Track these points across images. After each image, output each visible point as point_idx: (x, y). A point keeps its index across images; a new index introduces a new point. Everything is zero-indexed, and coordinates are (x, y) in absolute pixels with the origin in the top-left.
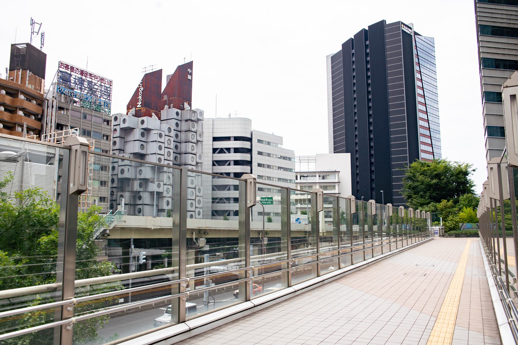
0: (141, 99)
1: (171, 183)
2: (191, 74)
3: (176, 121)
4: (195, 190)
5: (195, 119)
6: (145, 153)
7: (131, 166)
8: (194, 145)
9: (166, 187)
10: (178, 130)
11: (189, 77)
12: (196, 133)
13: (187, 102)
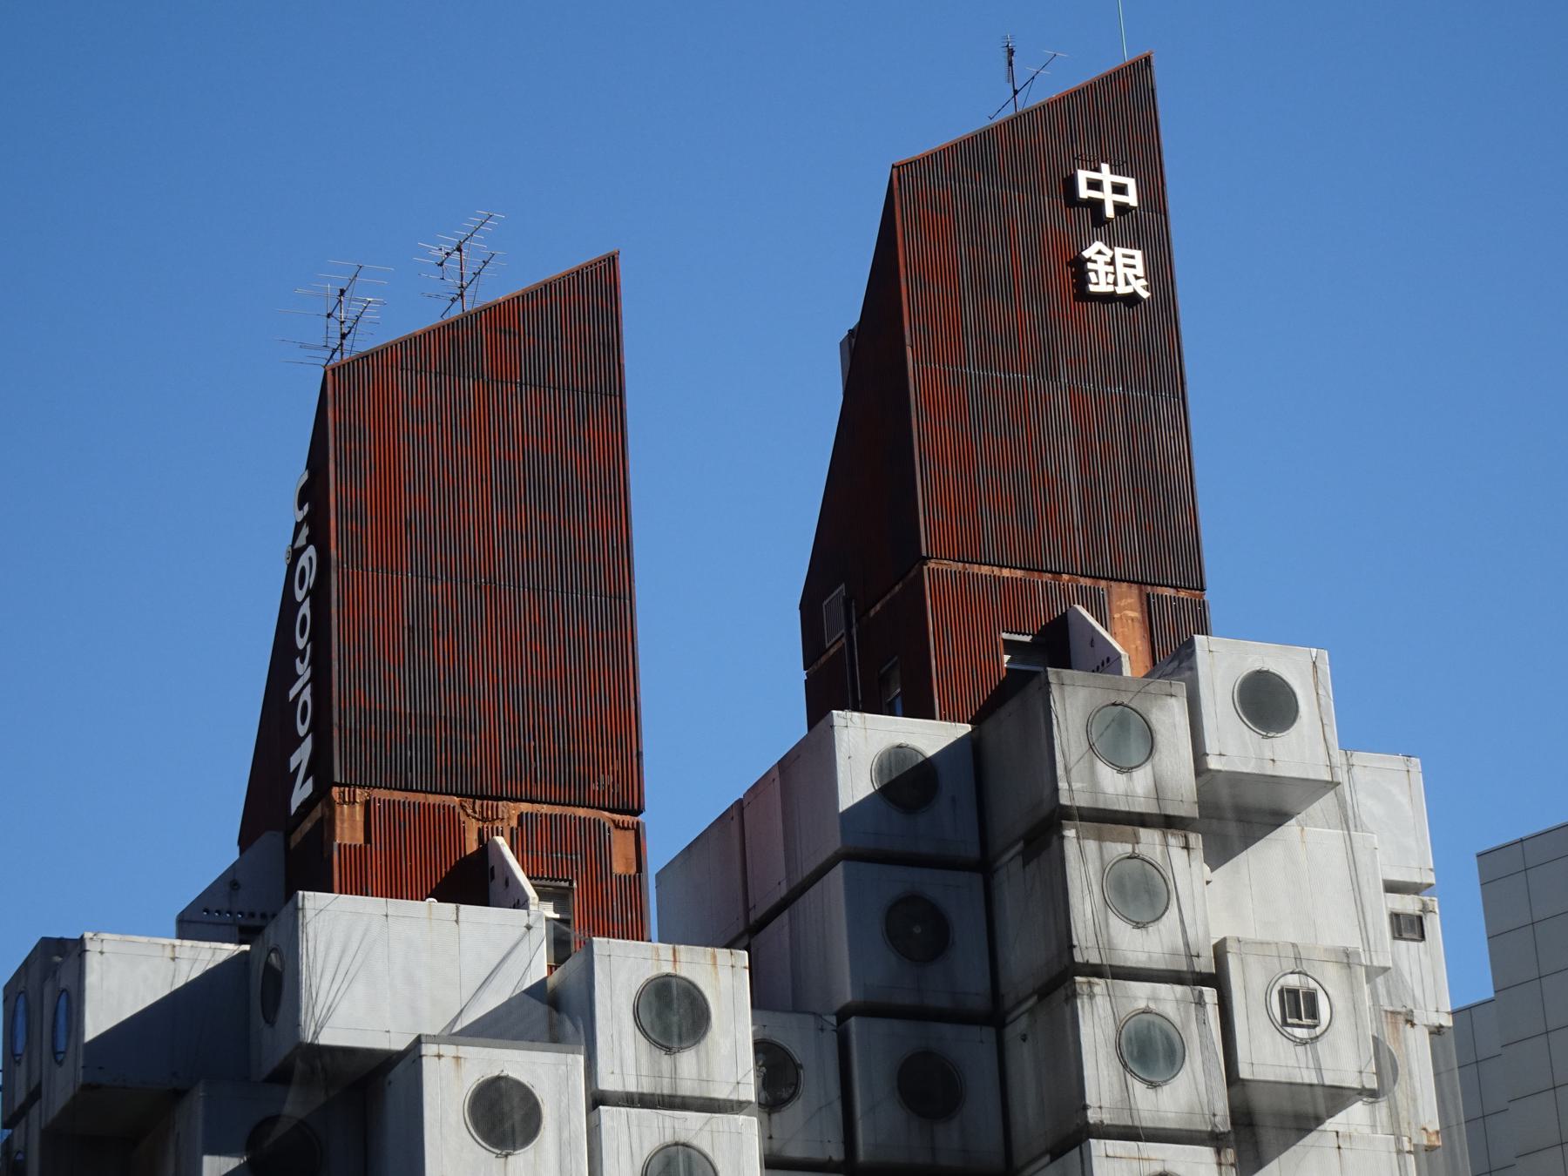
0: (306, 696)
3: (900, 880)
5: (1158, 791)
12: (1218, 980)
13: (1126, 604)
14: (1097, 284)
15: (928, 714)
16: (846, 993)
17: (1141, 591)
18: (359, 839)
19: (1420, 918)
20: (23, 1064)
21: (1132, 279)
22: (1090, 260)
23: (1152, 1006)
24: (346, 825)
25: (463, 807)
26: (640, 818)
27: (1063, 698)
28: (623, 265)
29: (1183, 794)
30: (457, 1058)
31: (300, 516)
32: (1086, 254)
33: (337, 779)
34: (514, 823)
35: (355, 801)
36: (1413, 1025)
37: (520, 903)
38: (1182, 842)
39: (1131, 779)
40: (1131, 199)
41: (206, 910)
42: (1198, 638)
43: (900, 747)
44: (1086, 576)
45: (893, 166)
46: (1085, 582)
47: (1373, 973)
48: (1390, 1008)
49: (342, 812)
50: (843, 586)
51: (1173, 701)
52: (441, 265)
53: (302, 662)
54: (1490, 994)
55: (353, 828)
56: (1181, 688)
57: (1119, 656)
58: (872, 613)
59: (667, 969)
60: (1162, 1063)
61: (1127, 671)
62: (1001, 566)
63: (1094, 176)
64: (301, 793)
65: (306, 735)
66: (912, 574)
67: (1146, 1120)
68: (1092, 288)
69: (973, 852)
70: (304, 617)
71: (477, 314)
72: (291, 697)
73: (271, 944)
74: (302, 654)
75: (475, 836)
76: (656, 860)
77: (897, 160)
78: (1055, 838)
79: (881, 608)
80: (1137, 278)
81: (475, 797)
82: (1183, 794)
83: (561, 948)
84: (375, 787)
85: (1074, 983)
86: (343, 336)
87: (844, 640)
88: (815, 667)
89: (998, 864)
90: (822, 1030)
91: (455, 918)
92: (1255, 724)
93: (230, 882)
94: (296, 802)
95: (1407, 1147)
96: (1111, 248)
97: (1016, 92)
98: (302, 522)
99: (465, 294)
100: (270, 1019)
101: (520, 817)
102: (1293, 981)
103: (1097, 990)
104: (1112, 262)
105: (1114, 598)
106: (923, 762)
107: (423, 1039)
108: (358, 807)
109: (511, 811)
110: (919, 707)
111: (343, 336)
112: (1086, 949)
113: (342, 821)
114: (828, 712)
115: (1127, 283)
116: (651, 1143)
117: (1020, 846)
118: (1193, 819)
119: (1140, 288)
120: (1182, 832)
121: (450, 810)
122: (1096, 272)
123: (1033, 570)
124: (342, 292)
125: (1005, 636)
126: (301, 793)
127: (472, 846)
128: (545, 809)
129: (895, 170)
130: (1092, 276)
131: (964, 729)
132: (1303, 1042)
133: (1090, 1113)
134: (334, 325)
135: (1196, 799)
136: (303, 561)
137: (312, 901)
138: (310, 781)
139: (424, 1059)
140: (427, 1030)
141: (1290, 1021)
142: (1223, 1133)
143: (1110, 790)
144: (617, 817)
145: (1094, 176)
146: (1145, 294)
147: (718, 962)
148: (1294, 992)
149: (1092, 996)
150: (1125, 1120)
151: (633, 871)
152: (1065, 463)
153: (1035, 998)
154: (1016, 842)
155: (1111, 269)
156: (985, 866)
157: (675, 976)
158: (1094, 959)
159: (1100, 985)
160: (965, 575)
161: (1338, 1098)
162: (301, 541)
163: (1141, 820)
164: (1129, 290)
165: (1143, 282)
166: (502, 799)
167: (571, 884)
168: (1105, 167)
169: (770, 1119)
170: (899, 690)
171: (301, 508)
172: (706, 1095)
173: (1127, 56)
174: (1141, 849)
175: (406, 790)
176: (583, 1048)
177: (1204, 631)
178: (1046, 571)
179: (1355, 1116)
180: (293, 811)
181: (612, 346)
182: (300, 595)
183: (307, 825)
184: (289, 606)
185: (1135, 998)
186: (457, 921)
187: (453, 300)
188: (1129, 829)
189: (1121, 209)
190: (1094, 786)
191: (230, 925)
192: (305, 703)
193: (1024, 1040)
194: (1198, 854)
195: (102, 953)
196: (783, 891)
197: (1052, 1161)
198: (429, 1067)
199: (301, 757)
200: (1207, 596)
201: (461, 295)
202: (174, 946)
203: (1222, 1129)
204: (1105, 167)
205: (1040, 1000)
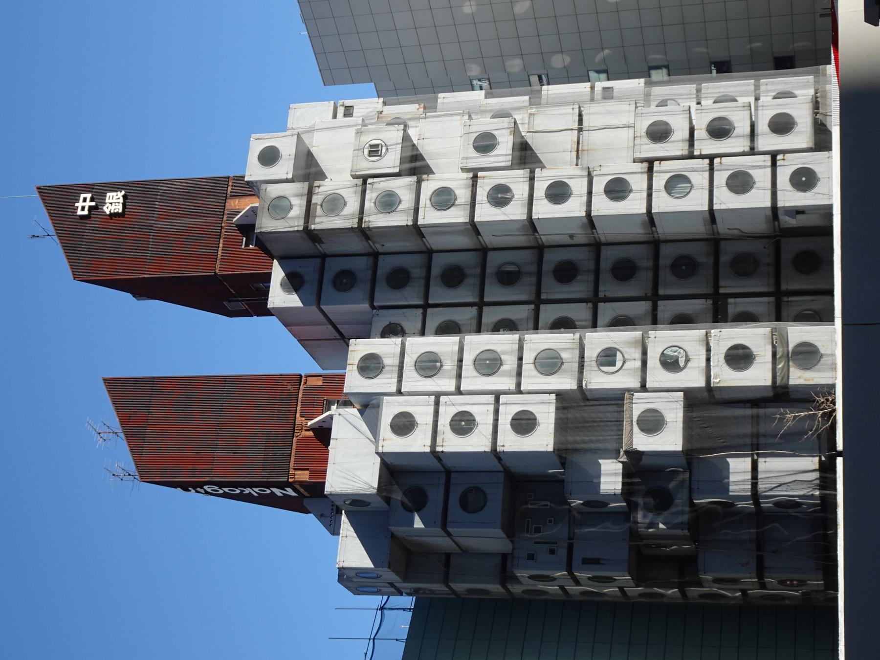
0: (257, 490)
1: (632, 343)
2: (99, 191)
3: (327, 287)
4: (661, 159)
6: (501, 477)
7: (570, 548)
8: (429, 187)
9: (658, 376)
10: (370, 272)
11: (114, 203)
12: (365, 179)
13: (233, 204)
14: (119, 209)
15: (271, 273)
16: (366, 306)
17: (229, 199)
18: (307, 472)
19: (346, 107)
20: (381, 588)
21: (117, 197)
22: (110, 211)
23: (373, 201)
24: (302, 477)
25: (297, 436)
26: (303, 375)
27: (265, 227)
28: (107, 376)
29: (301, 187)
30: (384, 440)
31: (193, 491)
33: (286, 480)
34: (303, 419)
35: (294, 474)
36: (382, 111)
37: (331, 417)
38: (317, 188)
39: (295, 205)
40: (89, 196)
41: (330, 525)
42: (246, 179)
43: (281, 285)
44: (223, 217)
45: (74, 279)
46: (225, 218)
47: (364, 124)
48: (376, 119)
49: (298, 478)
50: (224, 302)
51: (268, 189)
52: (105, 440)
53: (244, 491)
54: (373, 84)
55: (303, 474)
56: (263, 186)
57: (252, 207)
58: (234, 292)
59: (355, 367)
60: (393, 198)
61: (257, 205)
62: (219, 247)
63: (80, 209)
64: (290, 492)
65: (271, 490)
66: (220, 278)
67: (412, 205)
68: (120, 211)
69: (318, 261)
70: (229, 490)
71: (123, 428)
72: (257, 495)
73: (343, 503)
74: (242, 491)
75: (307, 432)
76: (320, 371)
77: (72, 278)
78: (314, 232)
79: (232, 289)
80: (117, 195)
81: (294, 432)
82: (301, 187)
83: (347, 404)
84: (289, 466)
85: (364, 228)
86: (129, 475)
87: (243, 303)
88: (252, 313)
89: (323, 253)
90: (378, 315)
91: (335, 440)
93: (321, 517)
94: (293, 494)
95: (424, 115)
97: (48, 235)
98: (195, 490)
99: (115, 432)
100: (367, 504)
101: (301, 417)
102: (366, 152)
103: (367, 220)
104: (111, 203)
105: (231, 208)
106: (287, 277)
107: (377, 452)
108: (296, 473)
109: (299, 420)
110: (267, 277)
111: (129, 475)
112: (354, 223)
113: (301, 478)
114: (268, 309)
115: (119, 199)
116: (415, 374)
117: (317, 244)
118: (309, 184)
119: (121, 194)
120: (314, 188)
121: (298, 441)
122: (115, 209)
123: (220, 236)
124: (114, 475)
125: (243, 246)
126: (290, 492)
127: (311, 433)
128: (299, 408)
129: (76, 279)
130: (116, 211)
131: (275, 261)
132: (387, 149)
133: (409, 224)
134: (125, 478)
135: (302, 183)
136: (209, 490)
137: (328, 489)
138: (286, 489)
139: (384, 451)
140: (374, 451)
141: (380, 154)
142: (417, 179)
143: (298, 213)
144: (302, 383)
145: (80, 209)
146: (123, 192)
147: (354, 350)
148: (370, 152)
149: (369, 222)
151: (321, 378)
152: (182, 223)
153: (369, 241)
154: (315, 245)
155: (113, 204)
156: (324, 257)
157: (358, 364)
158: (356, 220)
159: (365, 219)
160: (222, 260)
161: (406, 138)
162: (202, 491)
163: (309, 202)
165: (119, 193)
166: (295, 423)
167: (325, 400)
168: (77, 205)
169: (408, 333)
170: (261, 284)
171: (190, 491)
172: (399, 355)
173: (36, 195)
174: (319, 202)
175: (291, 456)
176: (382, 397)
177: (243, 177)
178: (221, 231)
179: (412, 133)
180: (297, 495)
181: (137, 381)
182: (221, 492)
183: (302, 490)
184: (225, 495)
185: (370, 206)
186: (337, 439)
187: (118, 436)
188: (312, 207)
189: (92, 200)
190: (297, 218)
191: (335, 517)
192: (259, 490)
193: (383, 245)
194: (321, 183)
195: (343, 561)
196: (330, 327)
197: (425, 238)
198: (386, 450)
199: (278, 492)
200: (231, 175)
201: (116, 433)
202: (342, 537)
203: (416, 179)
204: (77, 205)
205: (370, 239)
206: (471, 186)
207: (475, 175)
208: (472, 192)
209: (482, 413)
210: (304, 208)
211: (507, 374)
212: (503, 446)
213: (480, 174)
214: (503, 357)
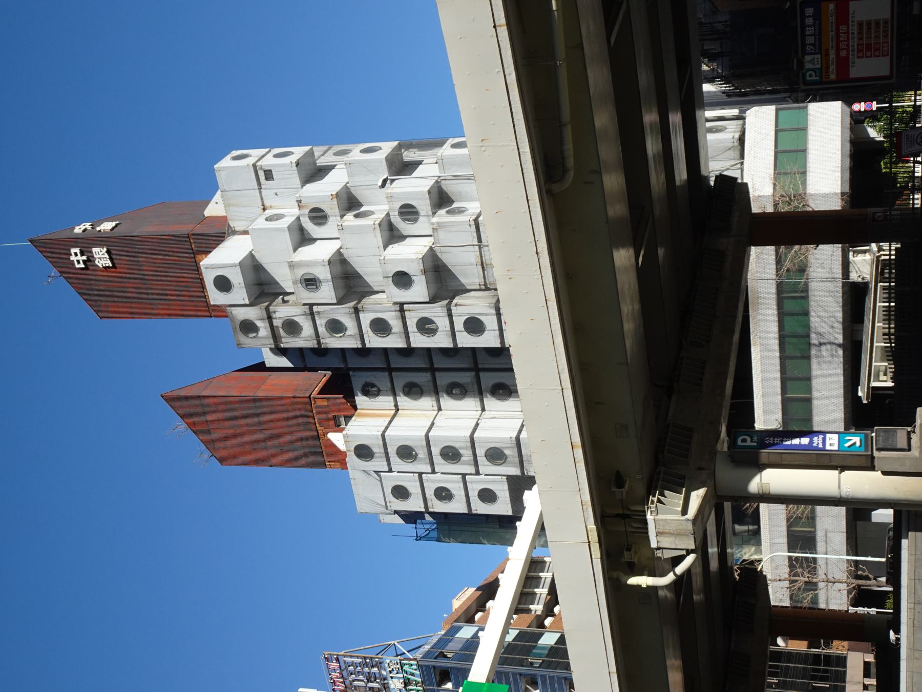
21: (102, 253)
22: (102, 265)
32: (101, 267)
34: (322, 428)
40: (77, 250)
92: (231, 289)
96: (95, 259)
103: (324, 342)
116: (398, 460)
130: (107, 265)
146: (105, 249)
149: (326, 343)
150: (358, 337)
164: (106, 254)
185: (323, 331)
206: (400, 318)
207: (401, 308)
208: (403, 322)
209: (456, 488)
210: (269, 329)
211: (465, 463)
212: (476, 510)
213: (405, 306)
214: (461, 451)
